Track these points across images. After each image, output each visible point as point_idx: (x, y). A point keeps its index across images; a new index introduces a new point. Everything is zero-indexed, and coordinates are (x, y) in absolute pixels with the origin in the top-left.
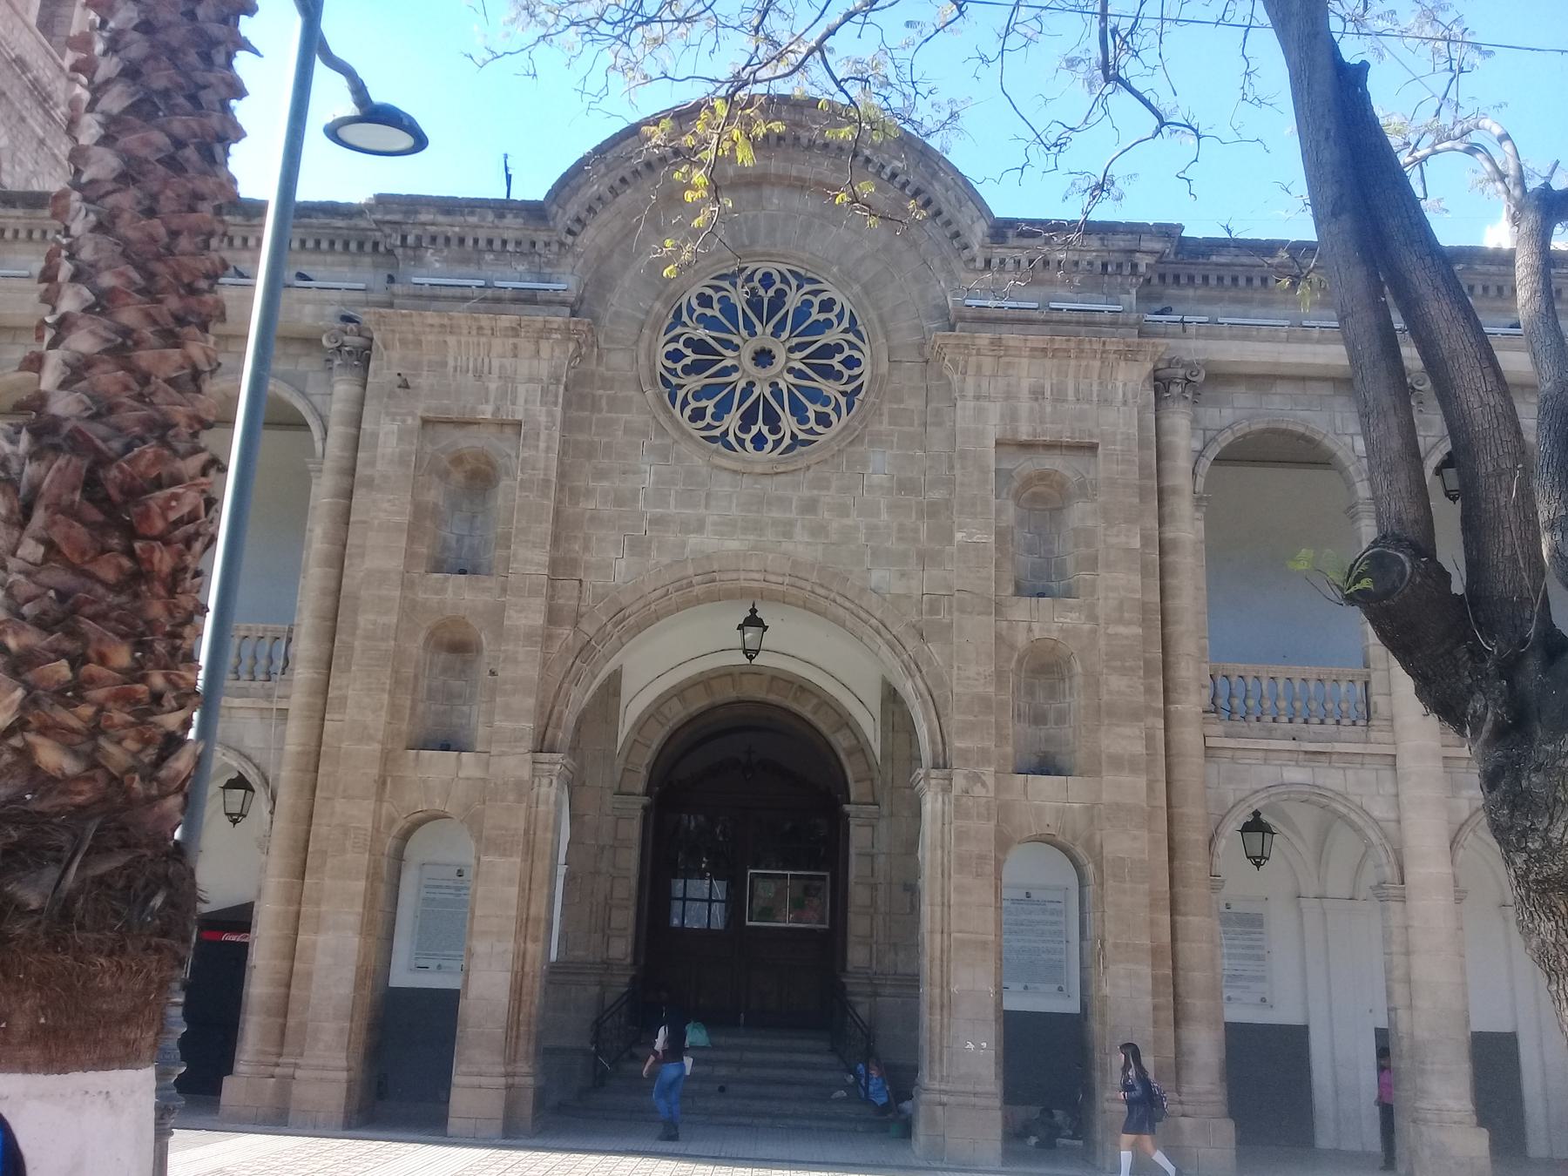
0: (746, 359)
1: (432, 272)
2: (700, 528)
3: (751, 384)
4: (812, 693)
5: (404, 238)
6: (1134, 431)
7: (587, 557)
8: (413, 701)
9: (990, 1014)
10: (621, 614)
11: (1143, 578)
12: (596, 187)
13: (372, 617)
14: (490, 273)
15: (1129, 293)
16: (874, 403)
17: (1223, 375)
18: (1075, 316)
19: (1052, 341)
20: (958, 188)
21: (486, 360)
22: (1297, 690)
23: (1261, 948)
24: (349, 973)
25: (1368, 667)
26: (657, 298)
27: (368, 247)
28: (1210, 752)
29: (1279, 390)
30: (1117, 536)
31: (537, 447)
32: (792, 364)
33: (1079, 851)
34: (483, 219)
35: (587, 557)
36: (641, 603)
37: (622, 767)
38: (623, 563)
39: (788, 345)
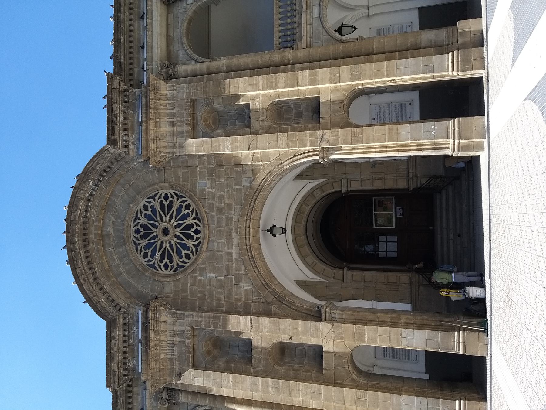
0: (165, 238)
5: (125, 375)
6: (185, 85)
7: (243, 300)
8: (303, 371)
12: (102, 300)
13: (270, 389)
14: (137, 341)
15: (135, 92)
18: (144, 112)
20: (97, 160)
21: (169, 342)
22: (283, 15)
24: (417, 400)
26: (144, 274)
27: (130, 389)
29: (172, 34)
31: (200, 321)
32: (167, 220)
36: (260, 277)
37: (333, 279)
38: (245, 285)
39: (160, 222)
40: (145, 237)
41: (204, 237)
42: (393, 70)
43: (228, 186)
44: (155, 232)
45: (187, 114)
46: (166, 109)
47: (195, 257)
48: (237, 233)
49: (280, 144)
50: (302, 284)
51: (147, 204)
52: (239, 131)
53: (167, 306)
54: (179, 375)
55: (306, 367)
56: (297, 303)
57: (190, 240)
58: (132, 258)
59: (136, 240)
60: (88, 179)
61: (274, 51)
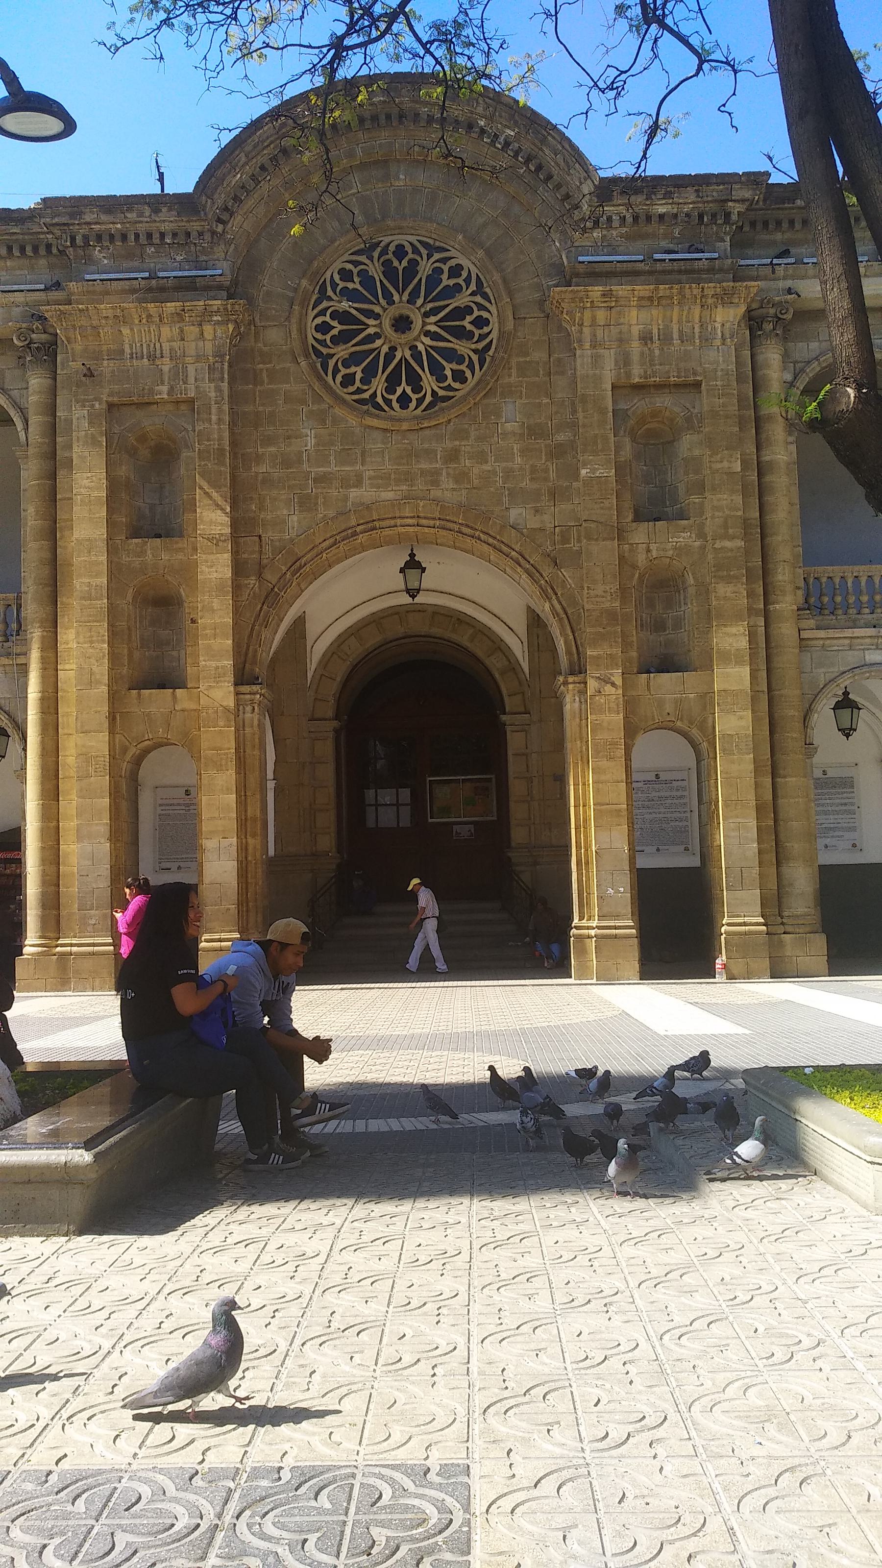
2: (359, 483)
3: (393, 349)
4: (468, 624)
6: (733, 367)
8: (129, 649)
12: (239, 176)
17: (810, 312)
19: (657, 289)
23: (852, 804)
27: (42, 251)
28: (804, 643)
30: (722, 462)
31: (210, 420)
32: (428, 328)
33: (695, 732)
34: (141, 215)
38: (295, 518)
39: (423, 310)
40: (389, 271)
43: (508, 474)
45: (668, 372)
46: (680, 322)
48: (406, 498)
51: (464, 274)
52: (628, 496)
55: (137, 654)
57: (386, 384)
59: (379, 249)
60: (519, 128)
61: (800, 567)
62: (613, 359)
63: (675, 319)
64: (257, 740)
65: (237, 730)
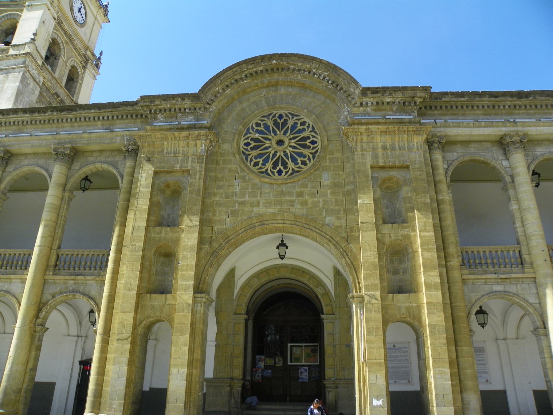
1: (161, 121)
2: (258, 205)
3: (276, 152)
6: (423, 159)
7: (215, 218)
9: (384, 393)
10: (228, 239)
11: (432, 214)
16: (323, 156)
17: (452, 142)
18: (395, 121)
21: (178, 149)
22: (494, 255)
23: (485, 360)
25: (520, 245)
27: (139, 116)
28: (464, 281)
30: (421, 198)
35: (215, 218)
36: (236, 234)
38: (229, 219)
39: (289, 138)
40: (276, 123)
41: (274, 179)
42: (440, 367)
44: (280, 132)
45: (395, 161)
46: (398, 141)
47: (256, 171)
48: (279, 211)
49: (366, 254)
50: (231, 274)
51: (307, 124)
53: (211, 146)
54: (149, 160)
56: (211, 270)
58: (254, 113)
62: (370, 155)
63: (396, 141)
64: (202, 321)
65: (192, 315)
